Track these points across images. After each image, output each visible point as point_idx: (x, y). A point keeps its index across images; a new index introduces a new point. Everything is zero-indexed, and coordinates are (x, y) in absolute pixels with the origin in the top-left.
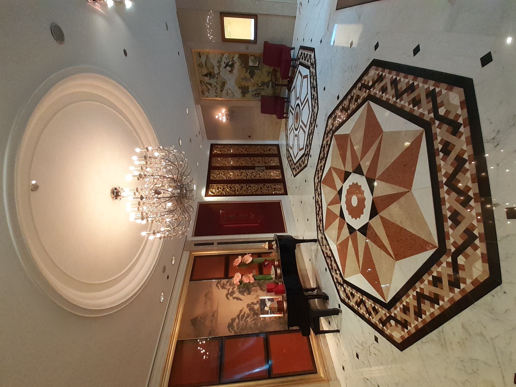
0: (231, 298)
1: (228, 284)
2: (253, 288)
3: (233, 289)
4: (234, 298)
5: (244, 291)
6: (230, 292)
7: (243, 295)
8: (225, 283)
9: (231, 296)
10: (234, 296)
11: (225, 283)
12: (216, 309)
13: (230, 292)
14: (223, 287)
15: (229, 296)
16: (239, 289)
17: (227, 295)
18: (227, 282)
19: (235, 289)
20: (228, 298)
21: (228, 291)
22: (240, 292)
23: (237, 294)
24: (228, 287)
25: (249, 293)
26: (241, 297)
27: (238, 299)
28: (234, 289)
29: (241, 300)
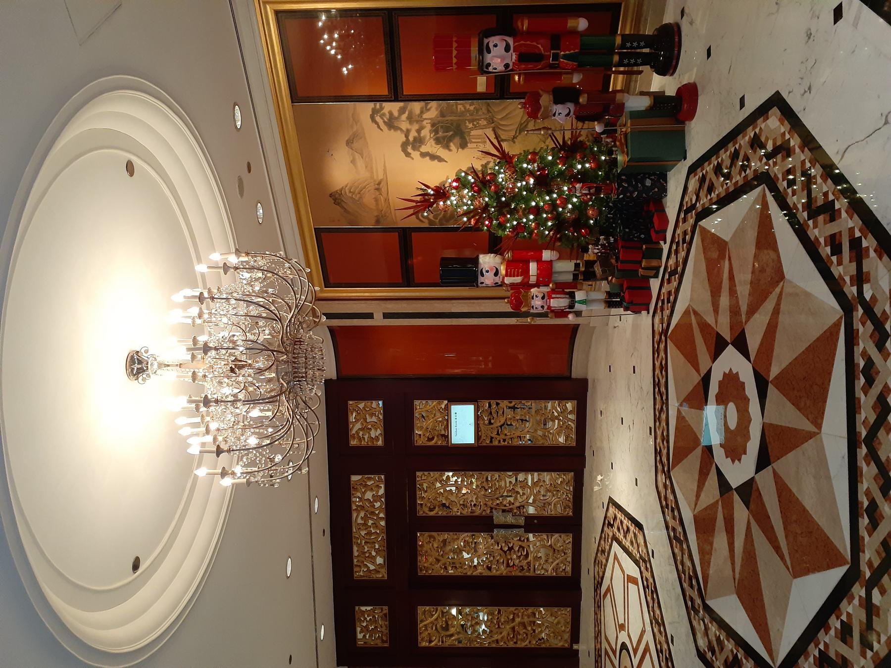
0: (415, 154)
1: (404, 117)
2: (473, 133)
3: (419, 131)
4: (423, 155)
5: (450, 139)
6: (411, 138)
7: (447, 147)
8: (396, 114)
9: (414, 148)
10: (424, 149)
11: (396, 114)
12: (381, 176)
13: (411, 138)
14: (391, 124)
15: (410, 150)
16: (436, 132)
17: (404, 146)
18: (402, 111)
19: (426, 133)
20: (408, 155)
21: (407, 136)
22: (438, 141)
23: (430, 146)
24: (404, 125)
25: (463, 145)
26: (441, 152)
27: (433, 157)
28: (423, 133)
29: (440, 159)
